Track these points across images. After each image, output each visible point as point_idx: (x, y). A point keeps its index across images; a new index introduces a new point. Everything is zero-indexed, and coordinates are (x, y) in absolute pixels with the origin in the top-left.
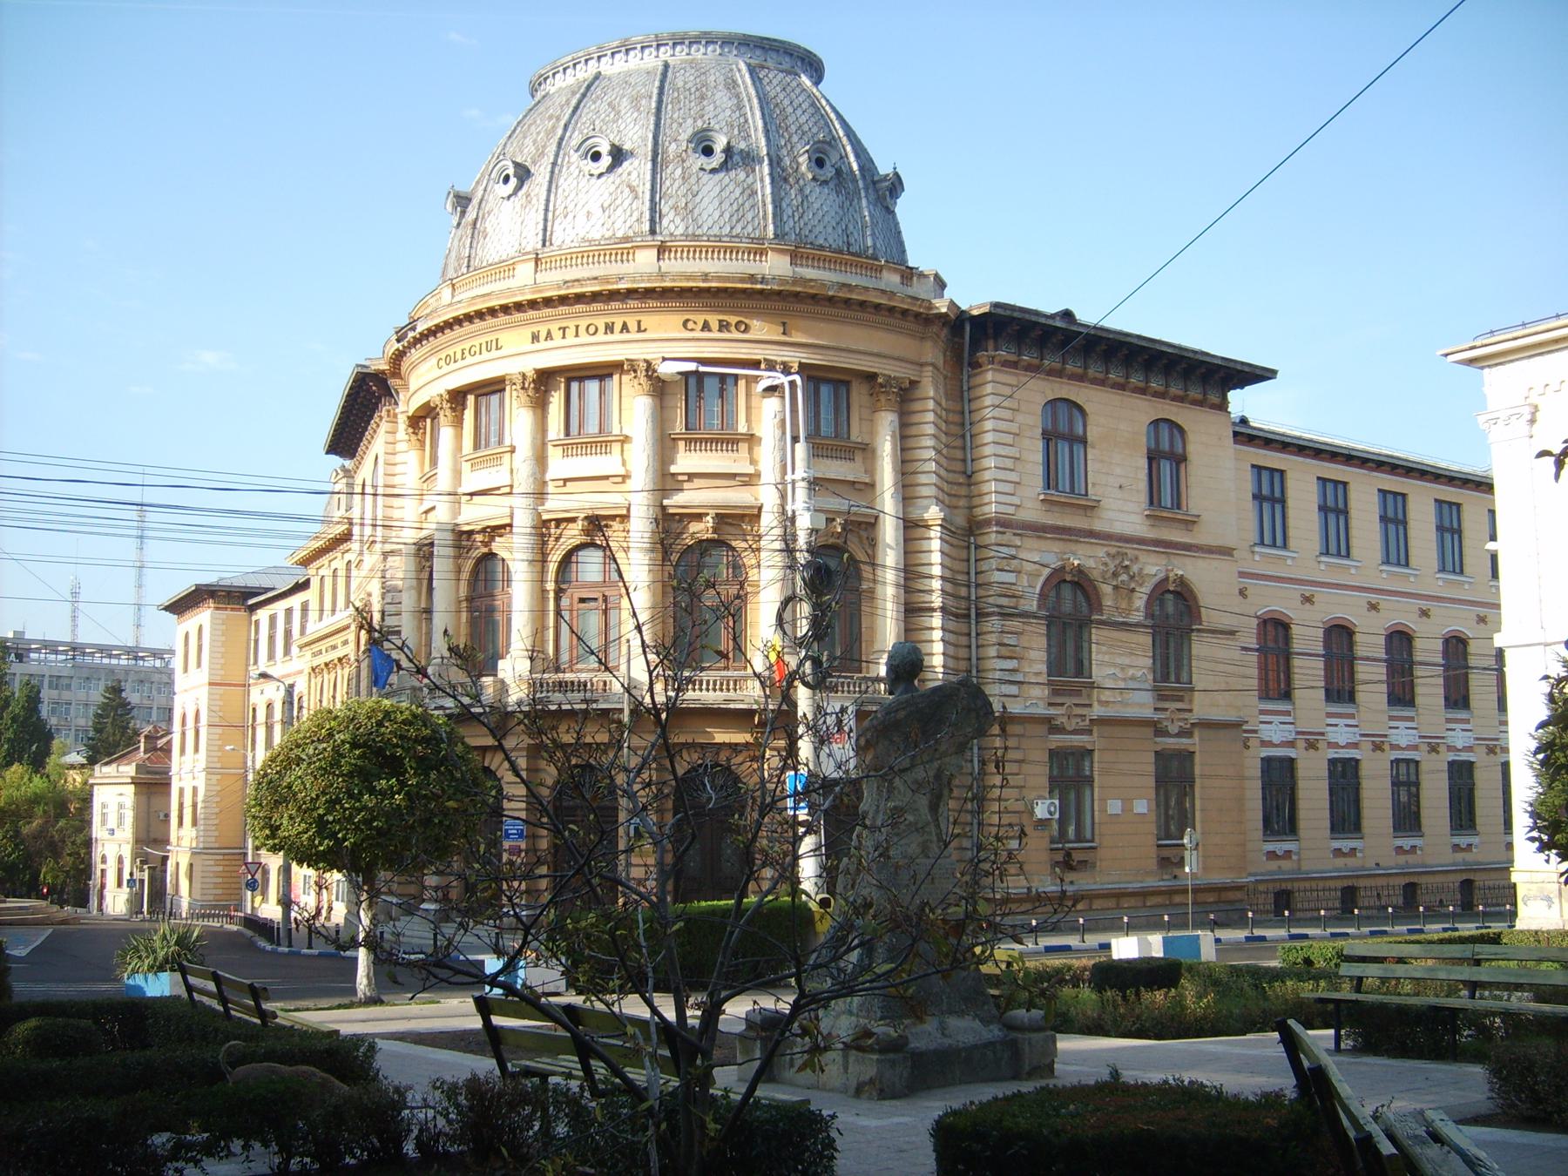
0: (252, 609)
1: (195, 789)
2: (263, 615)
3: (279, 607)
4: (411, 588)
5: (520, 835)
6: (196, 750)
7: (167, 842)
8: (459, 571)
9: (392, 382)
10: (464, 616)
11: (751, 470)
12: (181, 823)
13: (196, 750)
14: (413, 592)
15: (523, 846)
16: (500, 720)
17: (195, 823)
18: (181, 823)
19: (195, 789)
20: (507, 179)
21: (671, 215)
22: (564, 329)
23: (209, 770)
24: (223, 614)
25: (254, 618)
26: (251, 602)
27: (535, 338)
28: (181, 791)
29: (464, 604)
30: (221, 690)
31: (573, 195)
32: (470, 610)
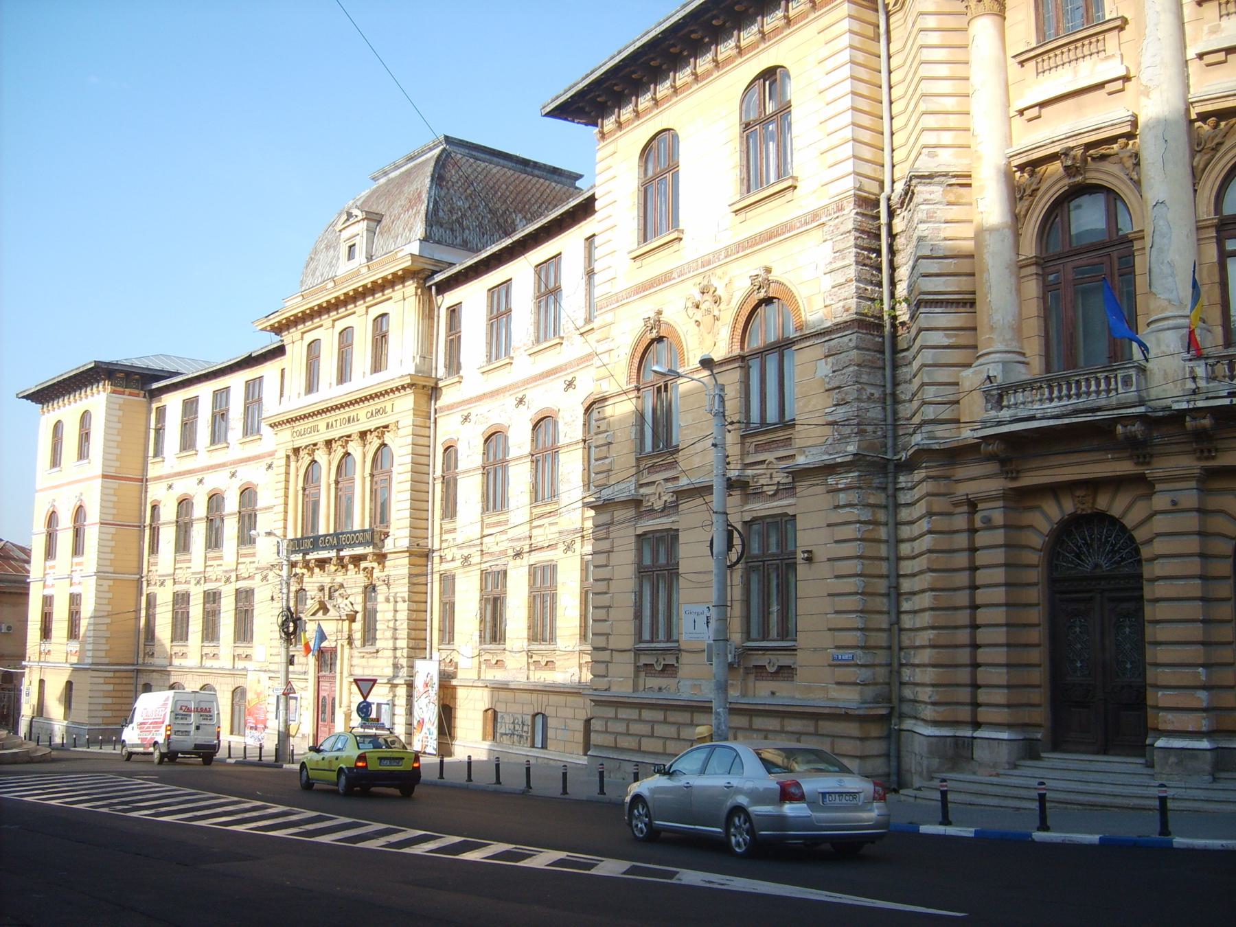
0: (154, 394)
1: (75, 599)
2: (173, 402)
3: (204, 391)
6: (77, 550)
7: (23, 657)
8: (1196, 175)
10: (1211, 252)
12: (46, 633)
13: (77, 550)
17: (73, 634)
18: (46, 633)
19: (75, 599)
23: (100, 575)
24: (120, 399)
25: (154, 406)
26: (155, 386)
28: (48, 601)
30: (114, 484)
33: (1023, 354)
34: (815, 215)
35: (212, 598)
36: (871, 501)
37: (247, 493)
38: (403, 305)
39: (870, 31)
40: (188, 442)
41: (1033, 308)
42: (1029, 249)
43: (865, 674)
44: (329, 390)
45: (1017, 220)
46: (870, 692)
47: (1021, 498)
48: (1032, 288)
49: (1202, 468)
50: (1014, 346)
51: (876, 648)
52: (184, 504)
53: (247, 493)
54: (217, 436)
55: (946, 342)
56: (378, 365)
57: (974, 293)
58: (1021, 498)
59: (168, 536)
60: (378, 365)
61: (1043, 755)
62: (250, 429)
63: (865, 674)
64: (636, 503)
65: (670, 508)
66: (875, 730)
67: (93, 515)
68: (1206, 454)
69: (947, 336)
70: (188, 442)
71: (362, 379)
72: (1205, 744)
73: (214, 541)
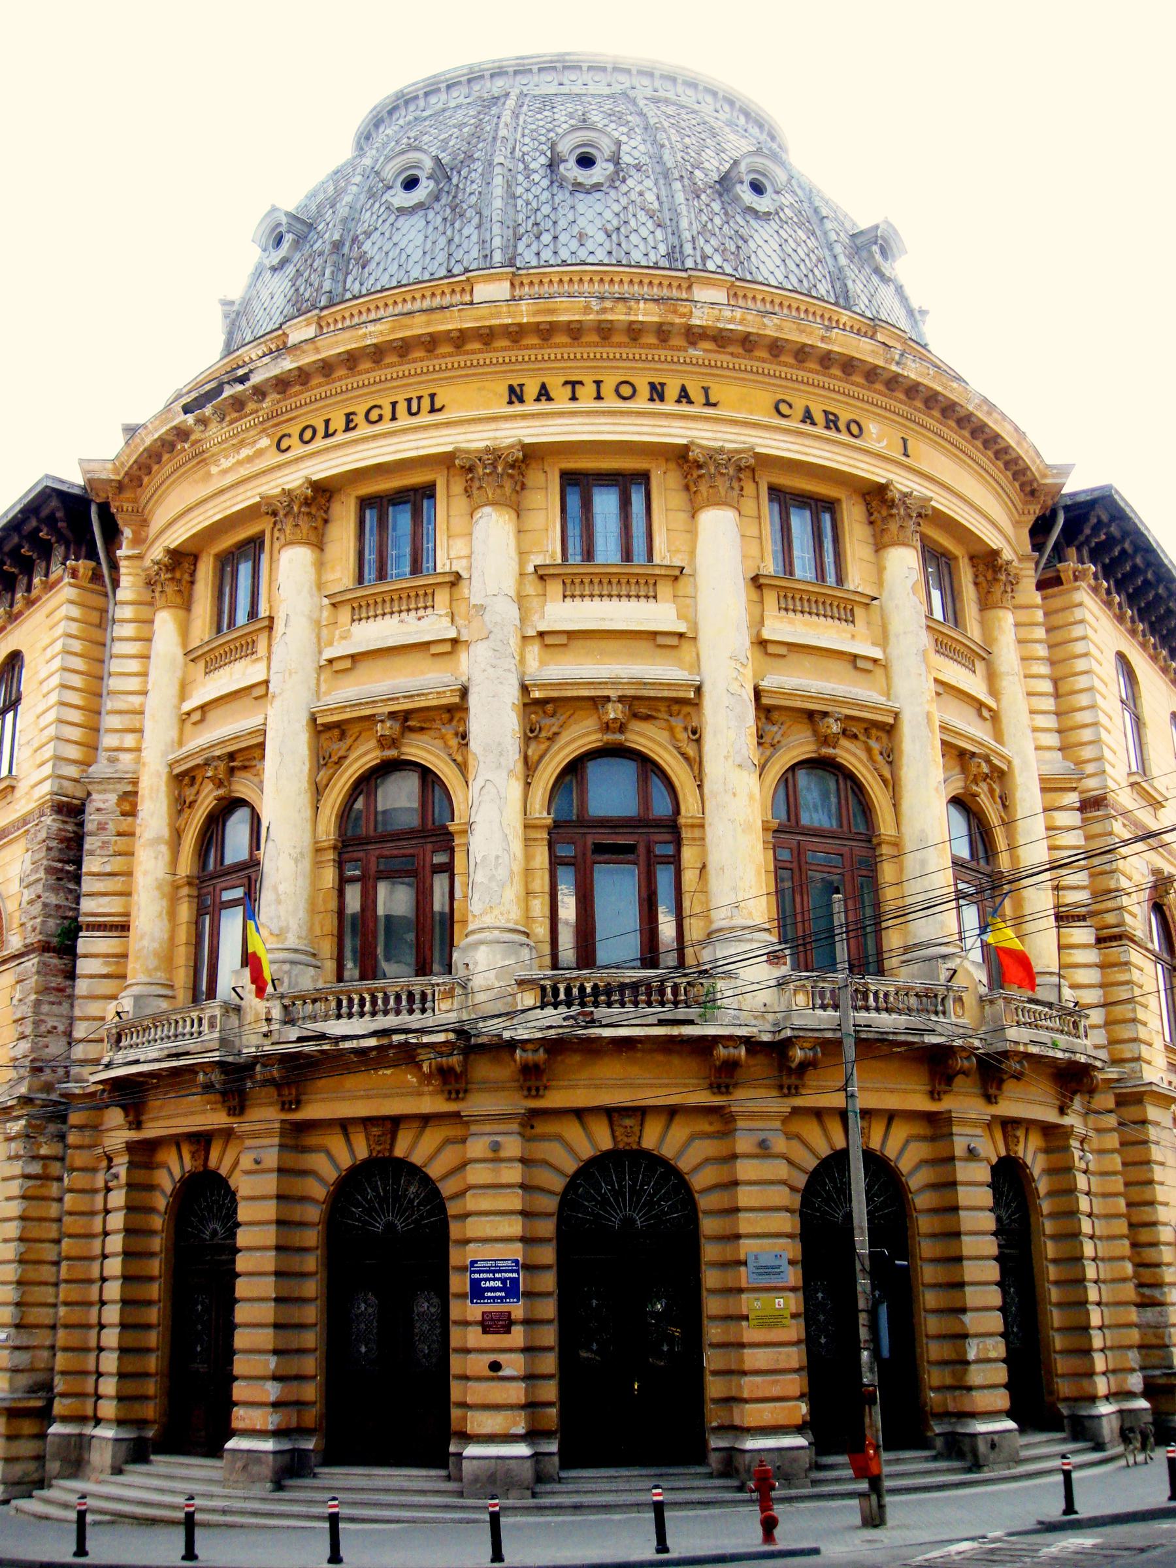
4: (157, 841)
5: (511, 1290)
8: (318, 791)
9: (121, 507)
11: (876, 653)
14: (164, 849)
15: (517, 1309)
16: (467, 1056)
20: (411, 184)
21: (718, 259)
22: (574, 384)
27: (516, 395)
29: (331, 855)
31: (546, 209)
32: (340, 864)
33: (171, 987)
34: (24, 821)
36: (43, 1151)
39: (95, 617)
41: (183, 934)
42: (186, 866)
43: (23, 1358)
45: (177, 835)
46: (24, 1380)
49: (283, 1121)
50: (160, 976)
51: (37, 1326)
55: (104, 971)
57: (128, 915)
58: (143, 1154)
61: (152, 1457)
63: (23, 1358)
66: (28, 1427)
68: (534, 1093)
69: (106, 964)
72: (269, 1445)
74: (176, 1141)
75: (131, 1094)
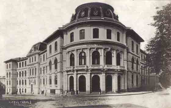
35: (23, 81)
37: (25, 71)
38: (37, 56)
40: (20, 66)
44: (31, 63)
47: (68, 75)
48: (69, 60)
52: (20, 72)
53: (25, 71)
54: (23, 66)
56: (35, 61)
59: (19, 75)
60: (35, 61)
62: (25, 66)
64: (54, 73)
65: (51, 75)
67: (11, 73)
70: (20, 66)
71: (34, 62)
73: (23, 76)
74: (70, 74)
75: (67, 71)
